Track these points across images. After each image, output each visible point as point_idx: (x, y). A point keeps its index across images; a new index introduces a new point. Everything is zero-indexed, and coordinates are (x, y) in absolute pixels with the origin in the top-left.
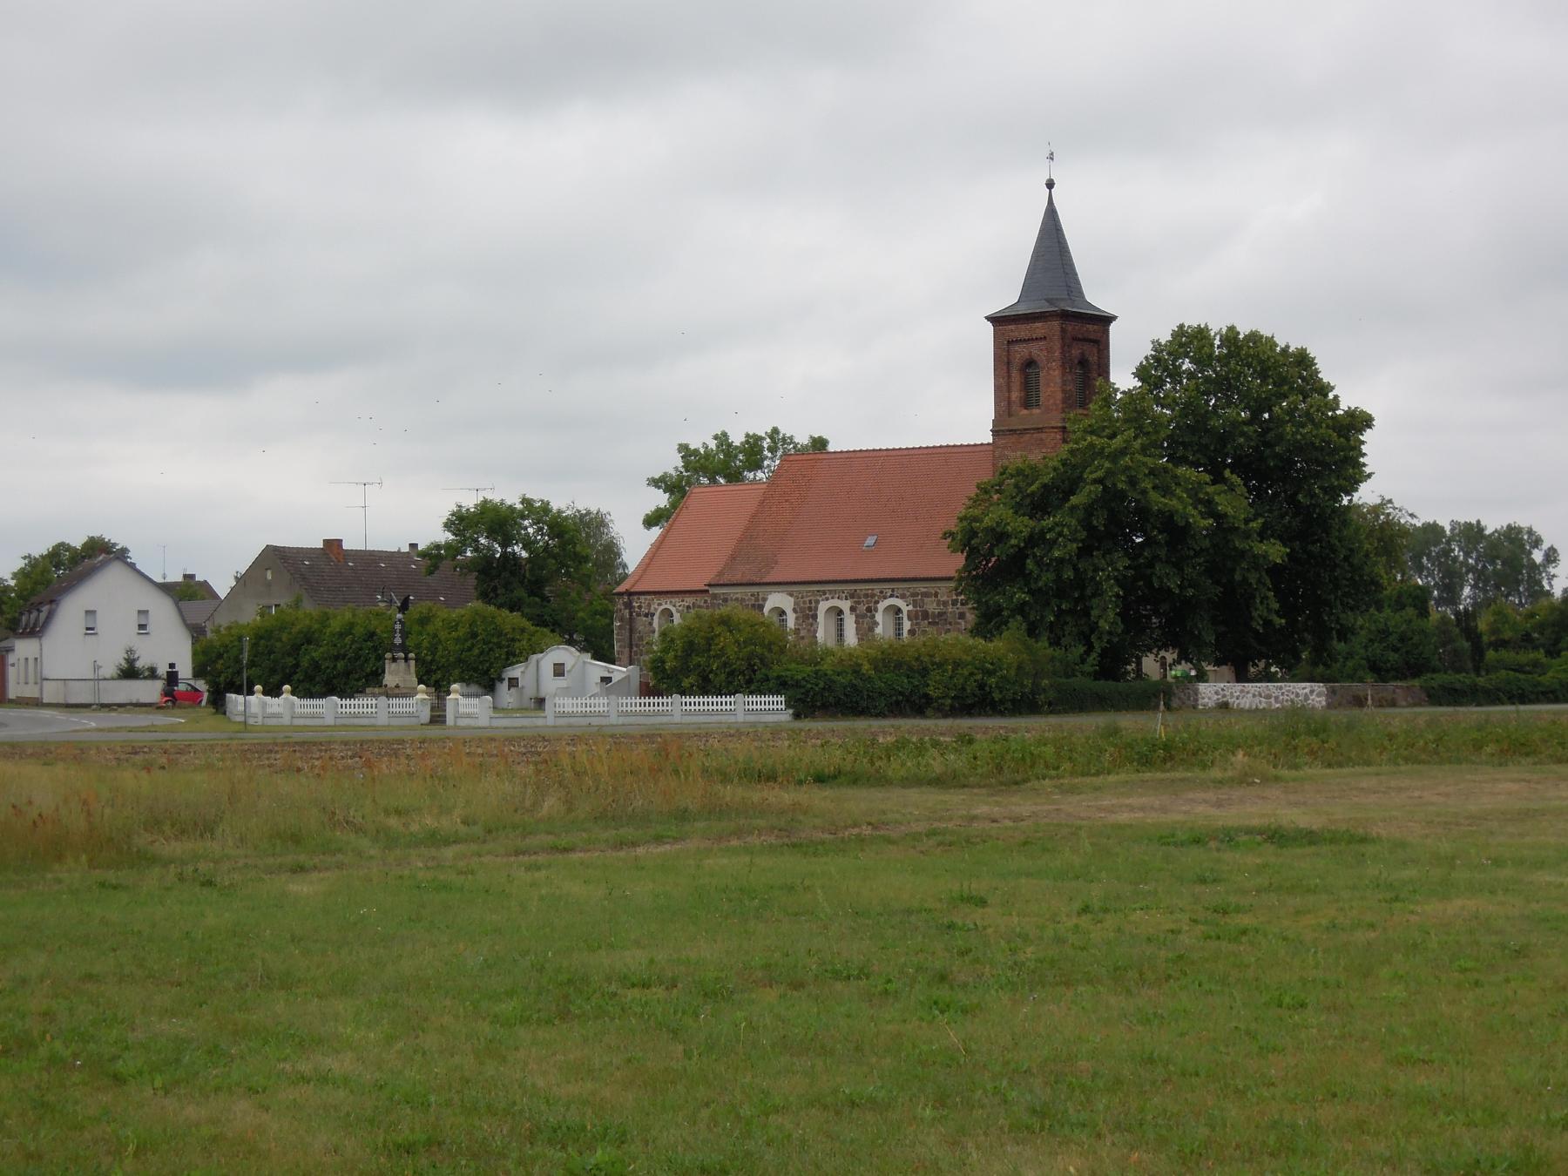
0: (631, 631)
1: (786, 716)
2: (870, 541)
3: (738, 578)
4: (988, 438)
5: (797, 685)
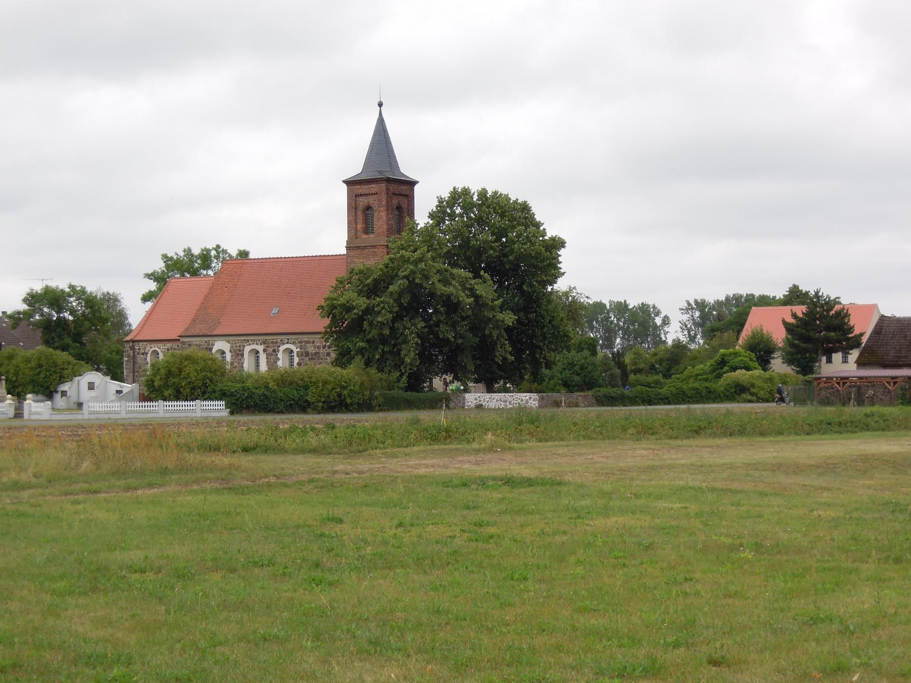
0: (134, 363)
1: (225, 413)
2: (275, 311)
3: (196, 332)
4: (344, 251)
5: (232, 394)
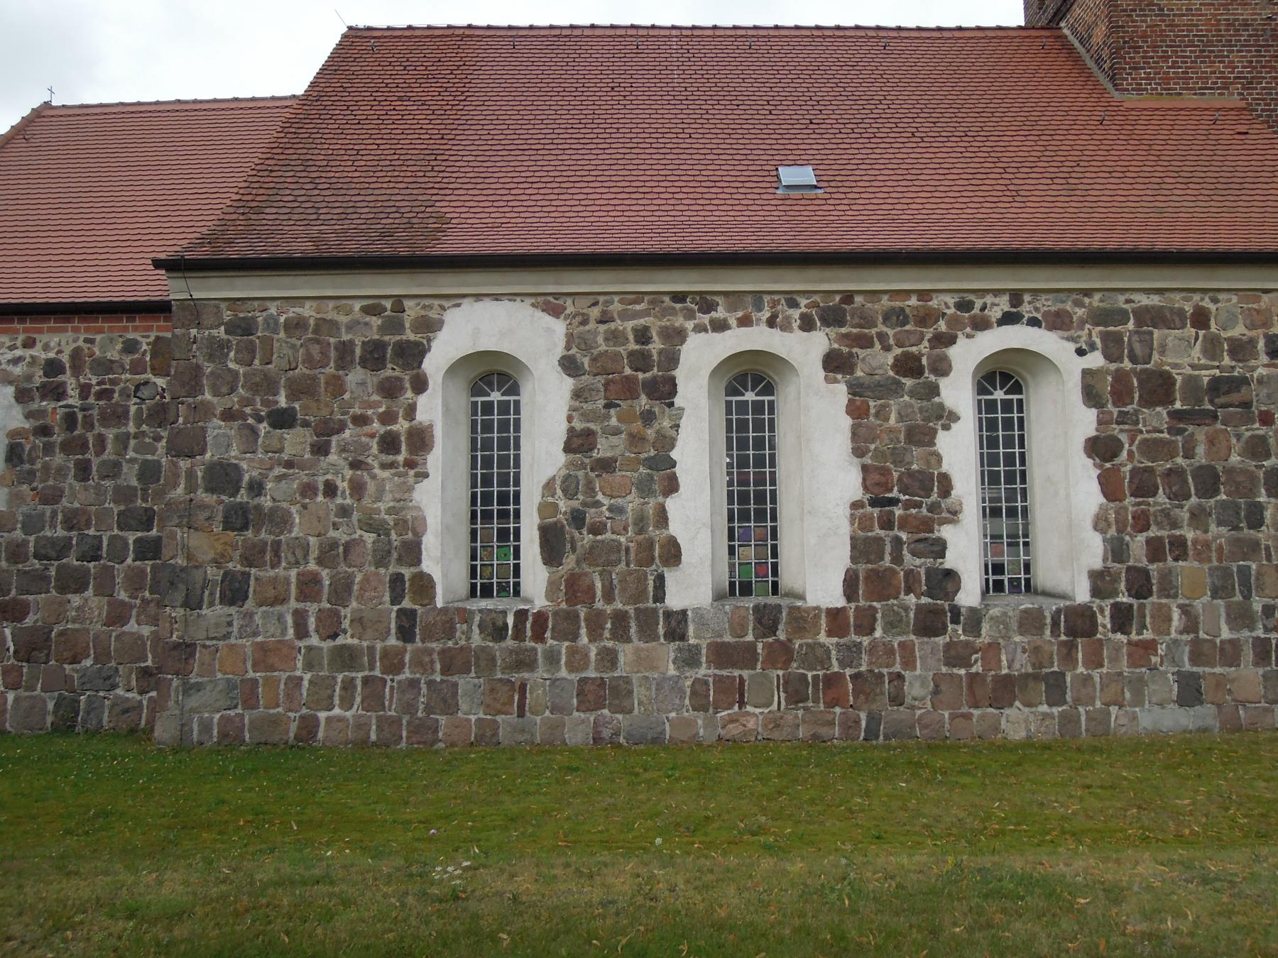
3: (301, 247)
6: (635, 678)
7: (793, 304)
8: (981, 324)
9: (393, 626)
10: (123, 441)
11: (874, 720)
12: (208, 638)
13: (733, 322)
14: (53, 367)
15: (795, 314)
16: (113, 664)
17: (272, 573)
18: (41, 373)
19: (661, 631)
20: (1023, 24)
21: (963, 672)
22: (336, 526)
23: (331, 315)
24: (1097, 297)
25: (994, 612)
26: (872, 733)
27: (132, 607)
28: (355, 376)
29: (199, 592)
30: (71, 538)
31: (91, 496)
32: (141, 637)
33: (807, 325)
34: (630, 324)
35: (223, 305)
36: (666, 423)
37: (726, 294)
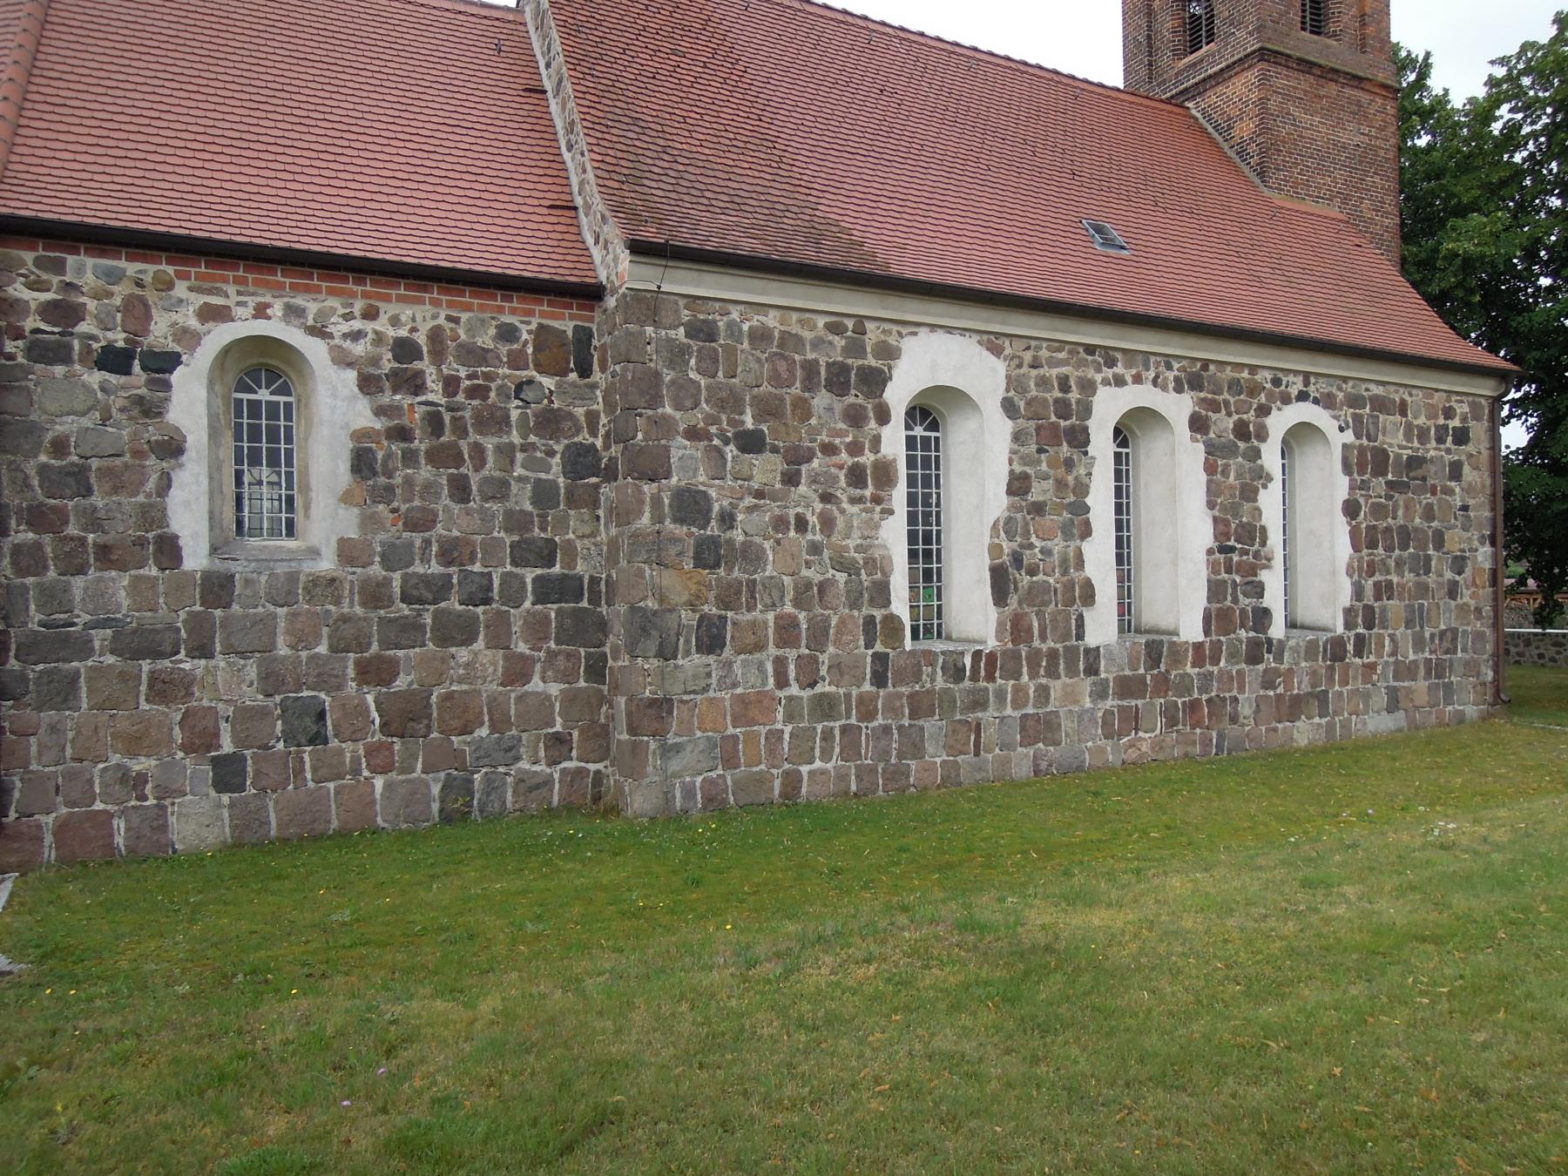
6: (1062, 712)
7: (1169, 367)
8: (1286, 400)
9: (868, 671)
10: (506, 453)
11: (1221, 736)
12: (686, 693)
13: (1129, 379)
14: (405, 350)
15: (1171, 375)
16: (514, 732)
17: (749, 617)
18: (390, 355)
19: (1082, 667)
20: (1121, 87)
21: (1272, 693)
22: (808, 565)
23: (796, 329)
24: (1351, 383)
25: (1292, 643)
26: (1219, 747)
27: (534, 661)
28: (821, 399)
29: (674, 639)
30: (450, 576)
31: (476, 521)
32: (548, 697)
33: (1179, 389)
34: (1055, 372)
35: (682, 302)
36: (1082, 471)
37: (1124, 351)
